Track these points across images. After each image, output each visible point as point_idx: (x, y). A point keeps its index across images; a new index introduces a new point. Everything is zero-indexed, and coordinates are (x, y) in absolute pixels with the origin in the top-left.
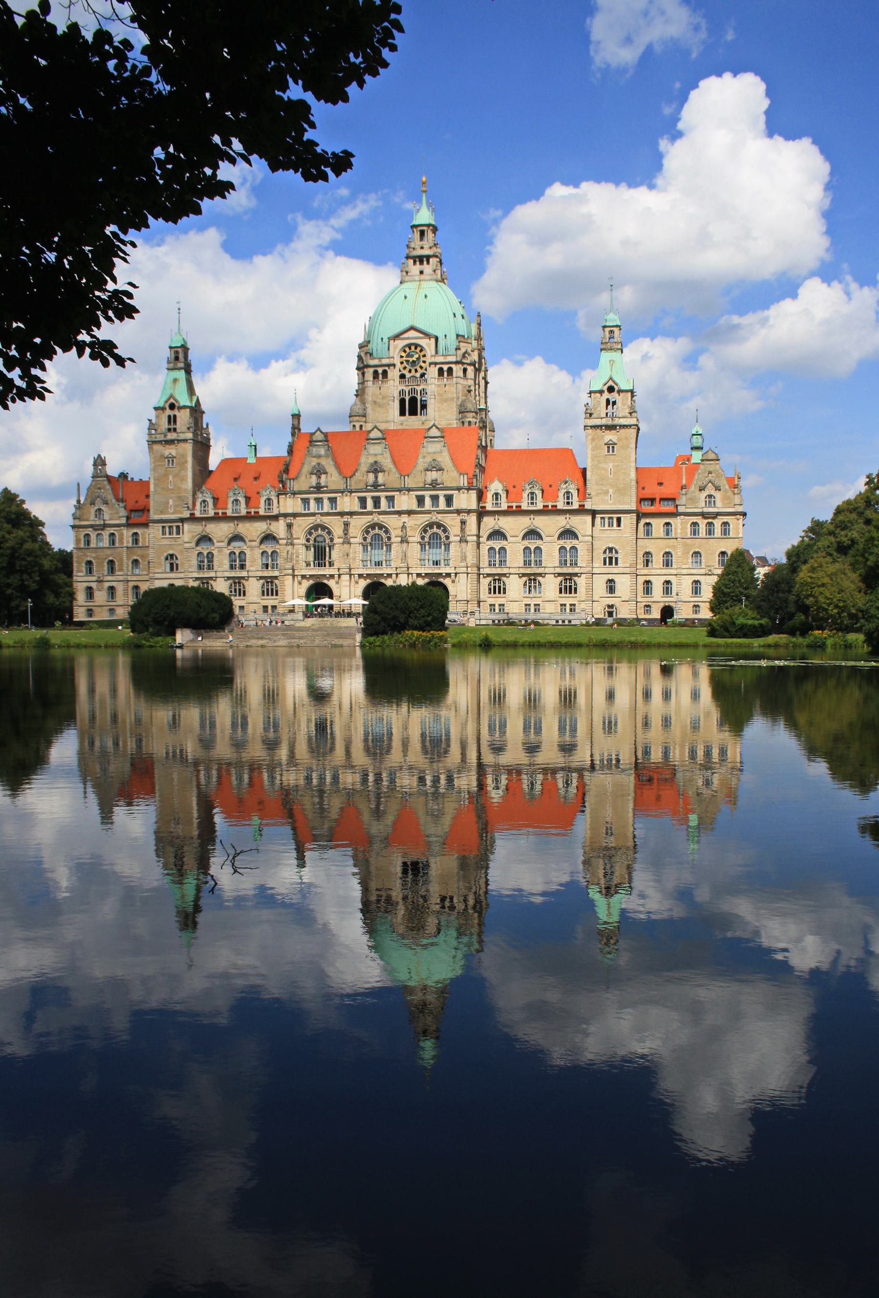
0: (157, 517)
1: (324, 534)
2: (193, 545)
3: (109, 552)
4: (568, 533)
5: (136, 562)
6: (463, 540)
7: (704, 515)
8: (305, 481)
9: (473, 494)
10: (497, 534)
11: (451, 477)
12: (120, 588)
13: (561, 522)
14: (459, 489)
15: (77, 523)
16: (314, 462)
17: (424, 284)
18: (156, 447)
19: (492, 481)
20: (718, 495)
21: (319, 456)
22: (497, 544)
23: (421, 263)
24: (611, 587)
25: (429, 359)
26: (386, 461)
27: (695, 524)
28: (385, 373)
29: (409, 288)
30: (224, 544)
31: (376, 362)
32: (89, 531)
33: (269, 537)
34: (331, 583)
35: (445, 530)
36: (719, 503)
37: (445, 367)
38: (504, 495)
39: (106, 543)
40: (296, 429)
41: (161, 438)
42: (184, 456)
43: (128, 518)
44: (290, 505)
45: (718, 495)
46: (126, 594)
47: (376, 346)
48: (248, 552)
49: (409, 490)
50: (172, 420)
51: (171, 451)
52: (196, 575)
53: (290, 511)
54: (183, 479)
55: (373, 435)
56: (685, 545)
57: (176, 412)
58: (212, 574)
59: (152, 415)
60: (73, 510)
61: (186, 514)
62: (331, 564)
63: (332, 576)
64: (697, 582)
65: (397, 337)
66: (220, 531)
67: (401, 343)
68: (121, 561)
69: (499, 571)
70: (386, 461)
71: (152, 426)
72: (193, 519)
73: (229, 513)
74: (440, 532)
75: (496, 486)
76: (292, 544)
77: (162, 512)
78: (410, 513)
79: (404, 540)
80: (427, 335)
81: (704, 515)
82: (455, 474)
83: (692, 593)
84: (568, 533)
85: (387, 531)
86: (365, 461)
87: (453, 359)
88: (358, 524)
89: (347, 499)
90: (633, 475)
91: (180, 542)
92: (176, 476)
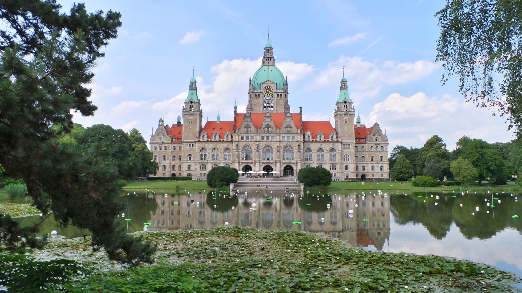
0: (185, 141)
1: (249, 148)
2: (199, 151)
3: (164, 153)
4: (333, 150)
5: (174, 156)
6: (299, 151)
7: (375, 144)
8: (243, 130)
9: (302, 136)
10: (309, 150)
11: (294, 129)
12: (167, 166)
13: (331, 146)
14: (297, 134)
15: (152, 142)
16: (246, 123)
17: (270, 67)
18: (186, 116)
19: (307, 132)
20: (379, 137)
21: (248, 122)
22: (309, 153)
23: (268, 60)
24: (347, 168)
25: (274, 91)
26: (272, 124)
27: (372, 147)
28: (259, 95)
29: (265, 68)
30: (210, 151)
31: (256, 91)
32: (156, 145)
33: (227, 149)
34: (252, 166)
35: (292, 148)
36: (380, 140)
37: (279, 94)
38: (311, 137)
39: (163, 149)
40: (235, 112)
41: (188, 113)
42: (196, 120)
43: (172, 141)
44: (236, 138)
45: (379, 137)
46: (170, 168)
47: (257, 87)
48: (219, 154)
49: (280, 134)
50: (191, 107)
51: (191, 118)
52: (224, 162)
53: (237, 140)
54: (196, 128)
55: (267, 115)
56: (369, 154)
57: (193, 104)
58: (206, 162)
59: (184, 105)
60: (150, 137)
61: (197, 140)
62: (252, 159)
63: (252, 163)
64: (373, 166)
65: (263, 83)
66: (209, 146)
67: (264, 86)
68: (168, 156)
69: (310, 162)
70: (272, 124)
71: (184, 109)
72: (199, 141)
73: (213, 140)
74: (290, 148)
75: (308, 133)
76: (238, 152)
77: (187, 139)
78: (280, 141)
79: (278, 151)
80: (274, 84)
81: (375, 144)
82: (296, 129)
83: (380, 170)
84: (333, 150)
85: (271, 148)
86: (264, 124)
87: (282, 91)
88: (262, 145)
89: (258, 137)
90: (354, 130)
91: (194, 150)
92: (193, 126)
